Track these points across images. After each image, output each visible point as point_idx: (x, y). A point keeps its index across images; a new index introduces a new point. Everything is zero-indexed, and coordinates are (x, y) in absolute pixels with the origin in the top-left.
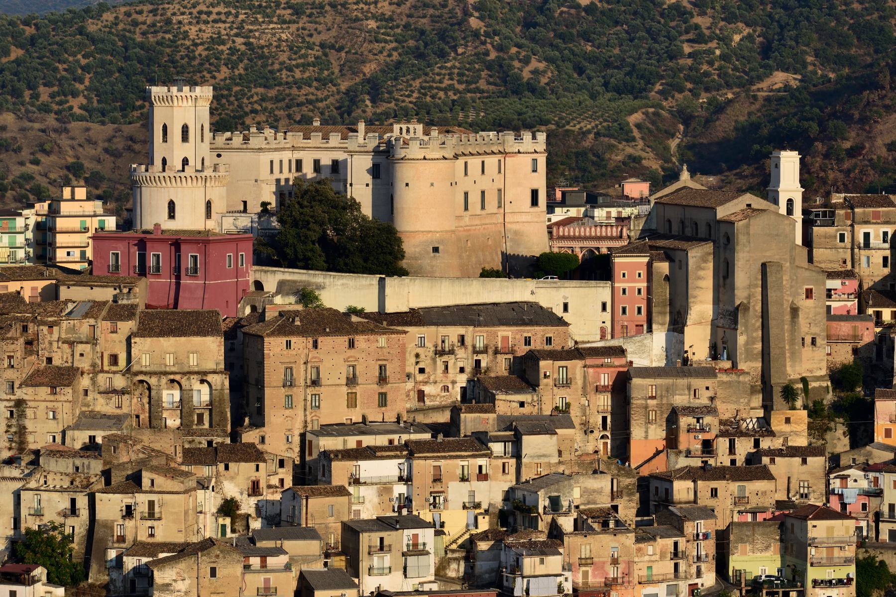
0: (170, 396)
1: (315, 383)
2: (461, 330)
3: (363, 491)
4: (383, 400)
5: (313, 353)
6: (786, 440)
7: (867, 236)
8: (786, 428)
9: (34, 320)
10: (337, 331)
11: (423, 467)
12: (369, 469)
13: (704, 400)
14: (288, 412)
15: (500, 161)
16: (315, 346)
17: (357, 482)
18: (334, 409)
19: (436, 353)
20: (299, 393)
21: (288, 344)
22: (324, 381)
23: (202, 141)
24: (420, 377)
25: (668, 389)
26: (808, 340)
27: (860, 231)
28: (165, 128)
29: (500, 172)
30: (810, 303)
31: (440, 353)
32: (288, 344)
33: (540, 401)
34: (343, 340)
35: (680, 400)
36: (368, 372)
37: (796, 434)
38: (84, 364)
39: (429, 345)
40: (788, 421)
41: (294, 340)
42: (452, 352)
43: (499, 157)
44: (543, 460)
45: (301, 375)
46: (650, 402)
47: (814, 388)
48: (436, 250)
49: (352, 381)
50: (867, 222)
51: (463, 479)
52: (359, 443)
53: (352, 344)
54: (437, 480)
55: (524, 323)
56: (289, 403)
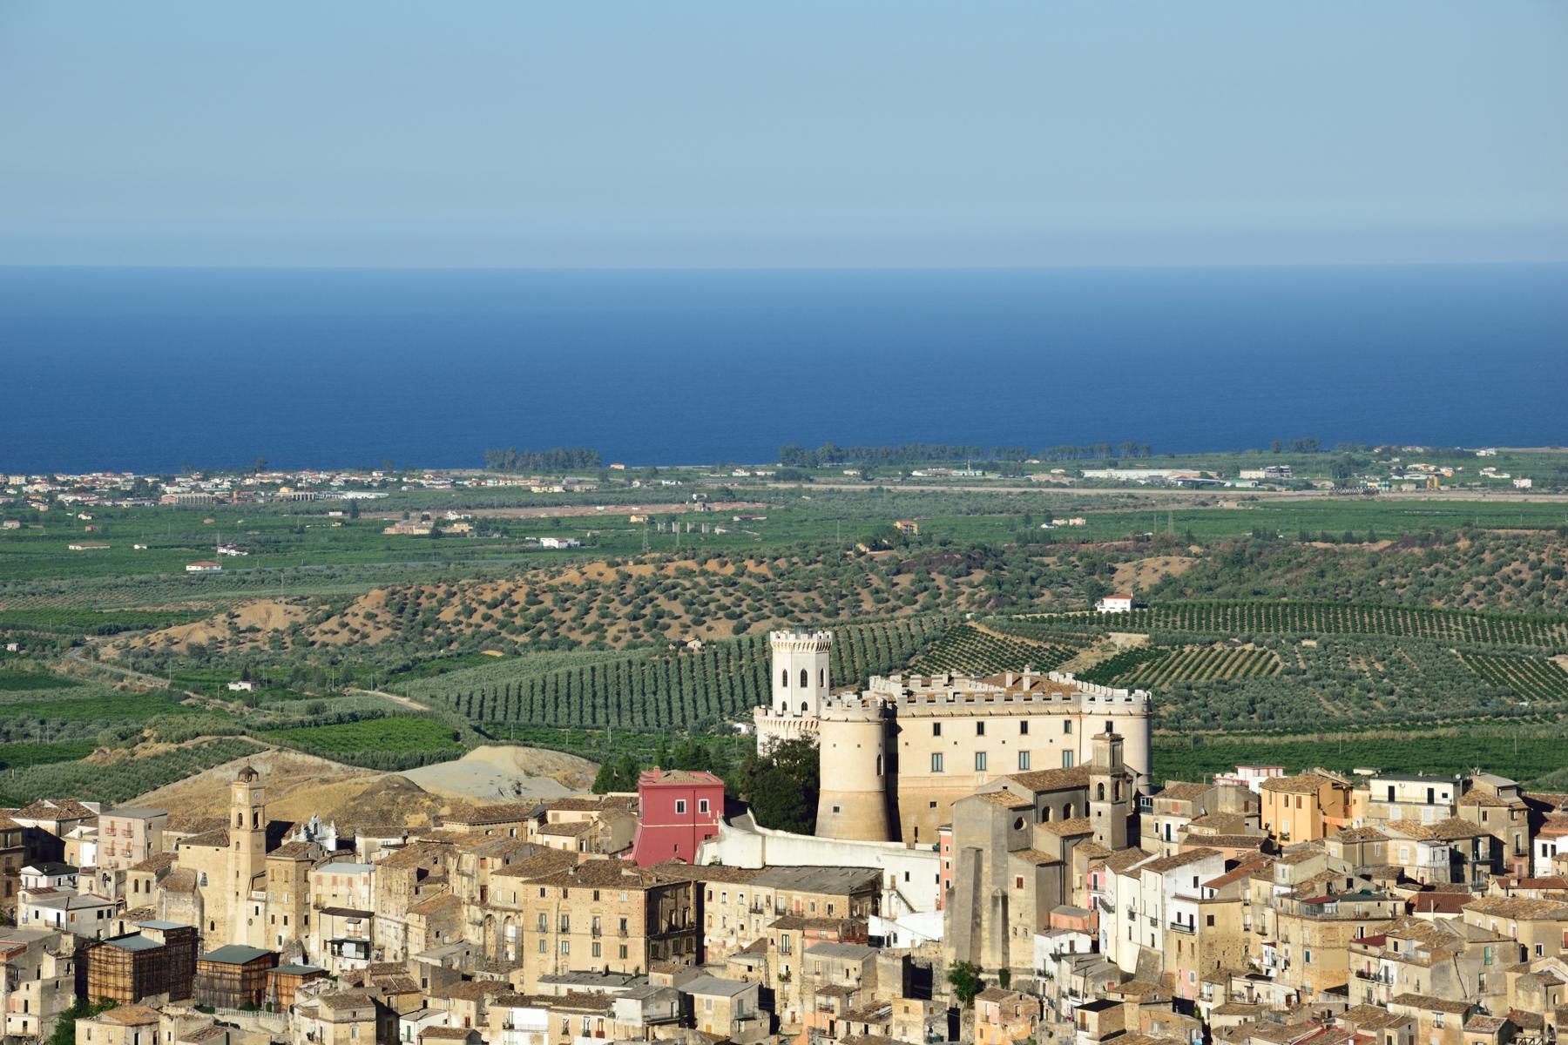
0: (511, 931)
1: (565, 930)
2: (770, 891)
3: (515, 1036)
4: (624, 952)
5: (563, 902)
6: (904, 1030)
7: (1168, 827)
8: (905, 1017)
9: (453, 853)
10: (586, 883)
11: (560, 1018)
12: (520, 1015)
13: (851, 983)
14: (542, 956)
15: (1067, 723)
16: (565, 896)
17: (511, 1027)
18: (581, 958)
19: (752, 911)
20: (551, 938)
21: (543, 893)
22: (572, 929)
23: (804, 683)
24: (741, 934)
25: (828, 966)
26: (1020, 930)
27: (1164, 821)
28: (785, 673)
29: (1067, 730)
30: (1020, 892)
31: (756, 910)
32: (543, 893)
33: (767, 966)
34: (590, 892)
35: (839, 979)
36: (610, 925)
37: (914, 1024)
38: (465, 896)
39: (746, 901)
40: (907, 1010)
41: (547, 888)
42: (761, 912)
43: (1067, 717)
44: (630, 1024)
45: (553, 924)
46: (818, 978)
47: (1019, 982)
48: (836, 809)
49: (596, 932)
50: (1168, 813)
51: (587, 1034)
52: (570, 990)
53: (596, 897)
54: (566, 1032)
55: (818, 889)
56: (542, 947)
